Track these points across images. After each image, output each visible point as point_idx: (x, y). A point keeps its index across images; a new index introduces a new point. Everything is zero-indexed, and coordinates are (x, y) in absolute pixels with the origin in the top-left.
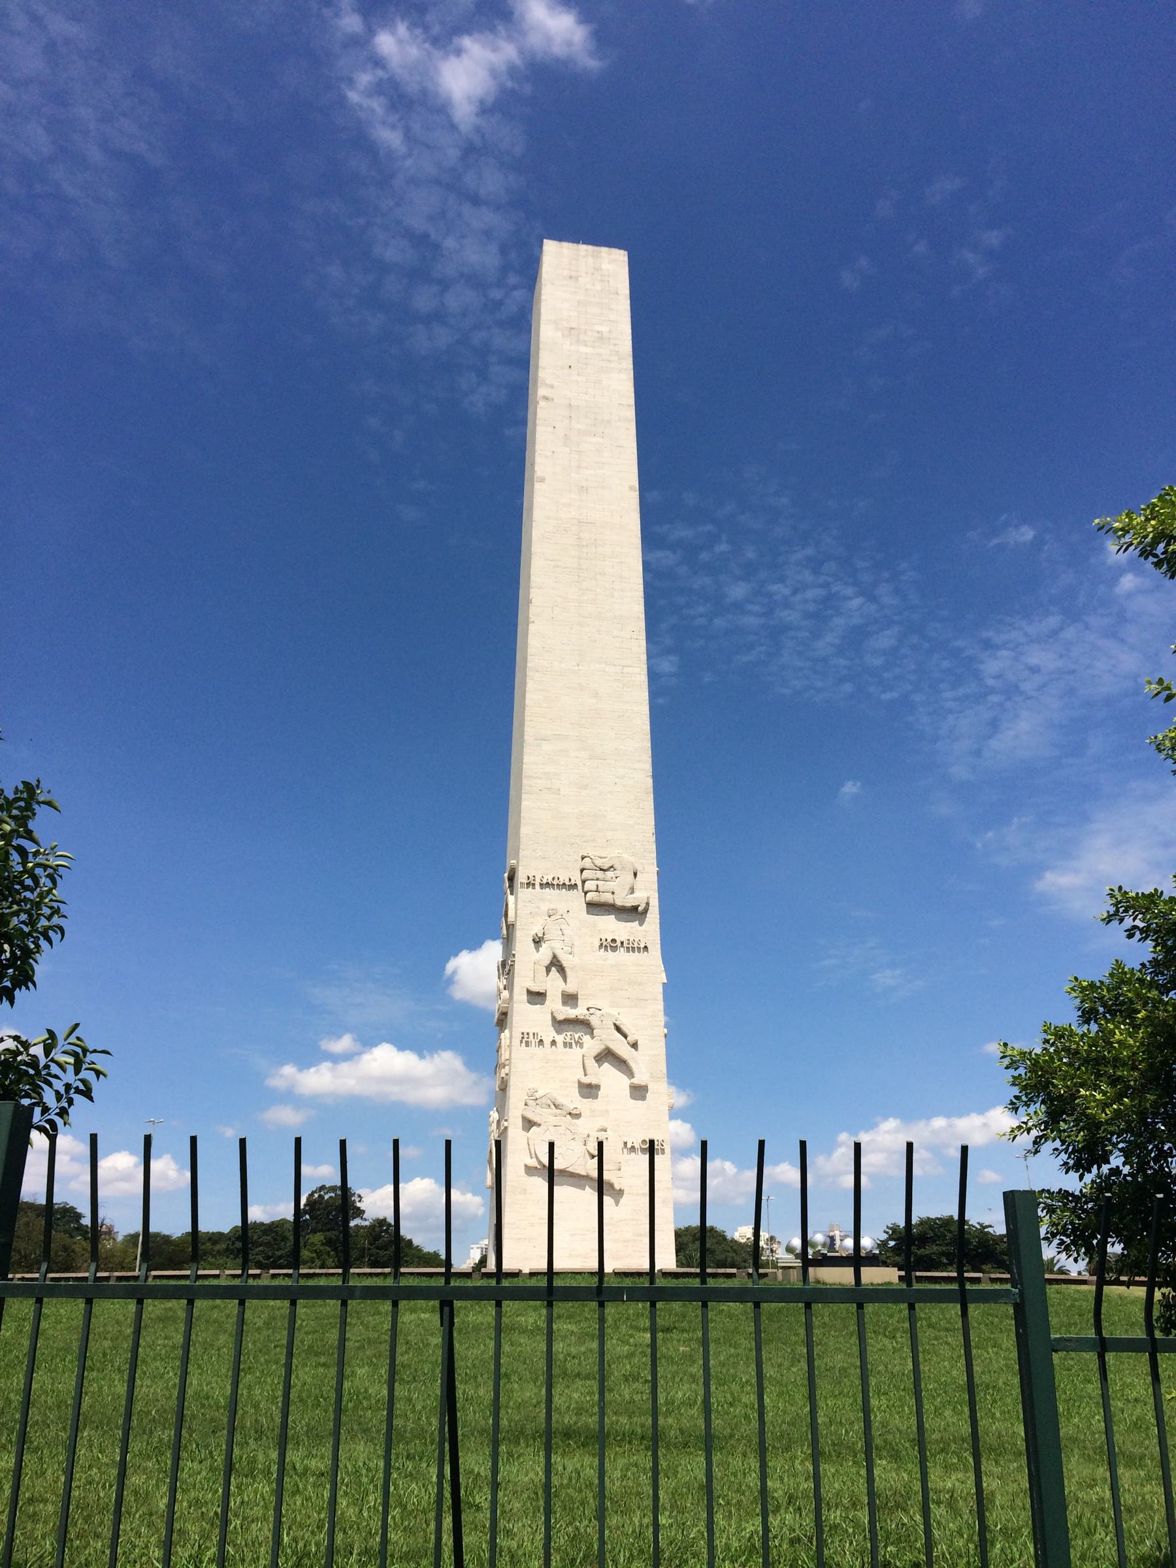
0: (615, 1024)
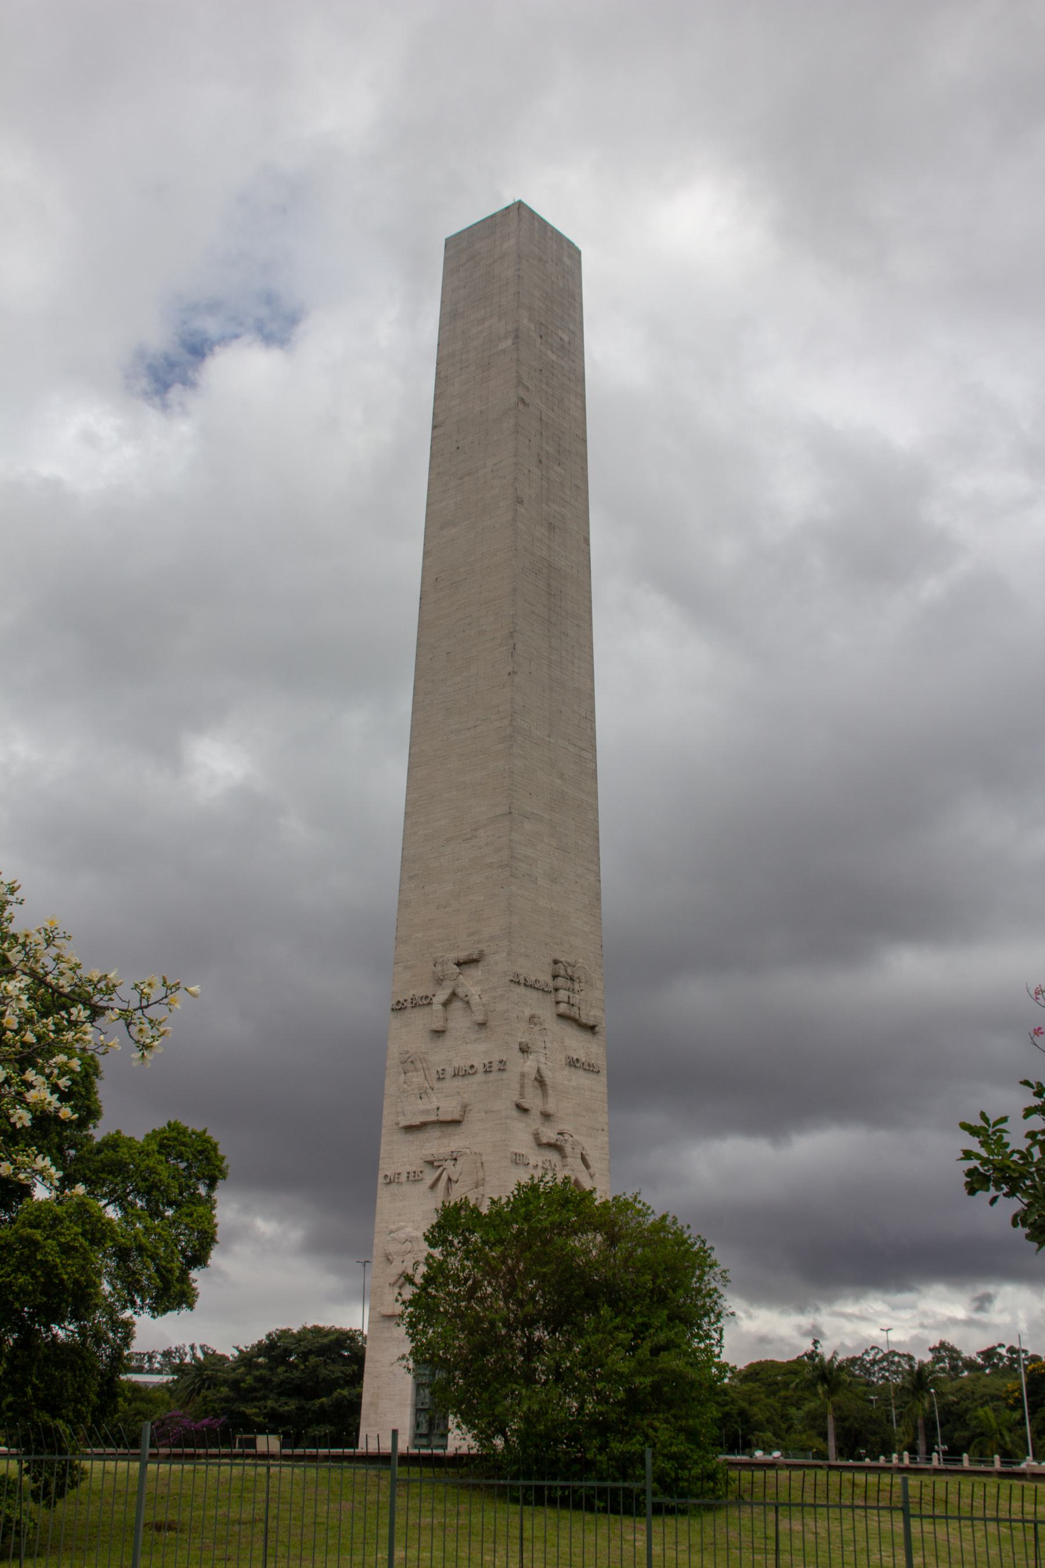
0: (582, 1154)
